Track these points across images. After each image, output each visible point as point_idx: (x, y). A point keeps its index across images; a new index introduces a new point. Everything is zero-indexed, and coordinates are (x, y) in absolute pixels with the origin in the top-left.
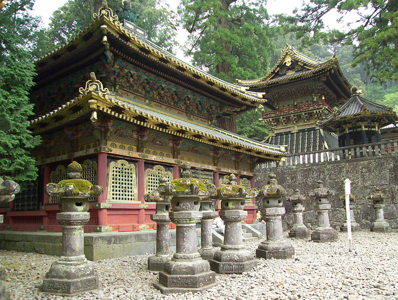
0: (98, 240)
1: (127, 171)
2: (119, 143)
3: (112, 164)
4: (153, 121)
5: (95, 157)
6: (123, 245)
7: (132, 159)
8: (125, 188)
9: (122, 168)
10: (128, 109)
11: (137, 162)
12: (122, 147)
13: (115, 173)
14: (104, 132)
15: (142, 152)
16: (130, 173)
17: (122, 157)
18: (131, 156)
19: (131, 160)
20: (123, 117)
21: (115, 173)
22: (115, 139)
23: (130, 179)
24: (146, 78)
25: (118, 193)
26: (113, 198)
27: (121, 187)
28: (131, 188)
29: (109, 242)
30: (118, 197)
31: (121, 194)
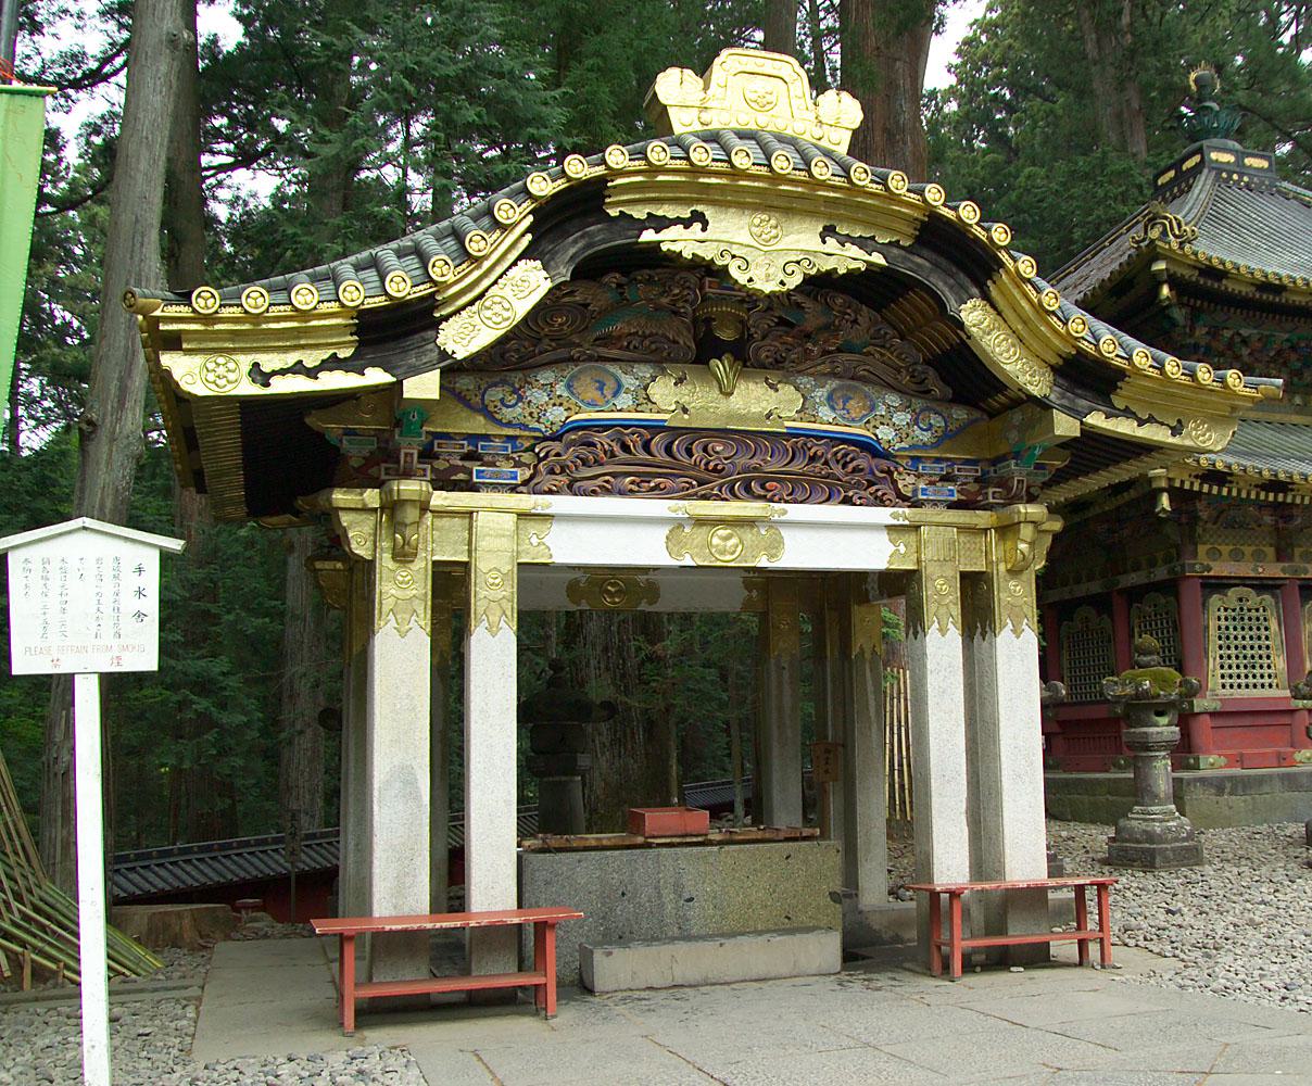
0: (1195, 786)
1: (1254, 613)
2: (1227, 545)
3: (1215, 600)
4: (1308, 486)
5: (1171, 587)
6: (1253, 799)
7: (1265, 582)
8: (1253, 657)
9: (1242, 609)
10: (1241, 473)
11: (1278, 587)
12: (1237, 556)
13: (1223, 623)
14: (1187, 524)
15: (1291, 559)
16: (1262, 618)
17: (1237, 582)
18: (1262, 575)
19: (1262, 586)
20: (1230, 491)
21: (1223, 623)
22: (1215, 536)
23: (1263, 633)
24: (1286, 336)
25: (1234, 671)
26: (1224, 686)
27: (1241, 656)
28: (1268, 657)
29: (1220, 790)
30: (1235, 681)
31: (1243, 675)
